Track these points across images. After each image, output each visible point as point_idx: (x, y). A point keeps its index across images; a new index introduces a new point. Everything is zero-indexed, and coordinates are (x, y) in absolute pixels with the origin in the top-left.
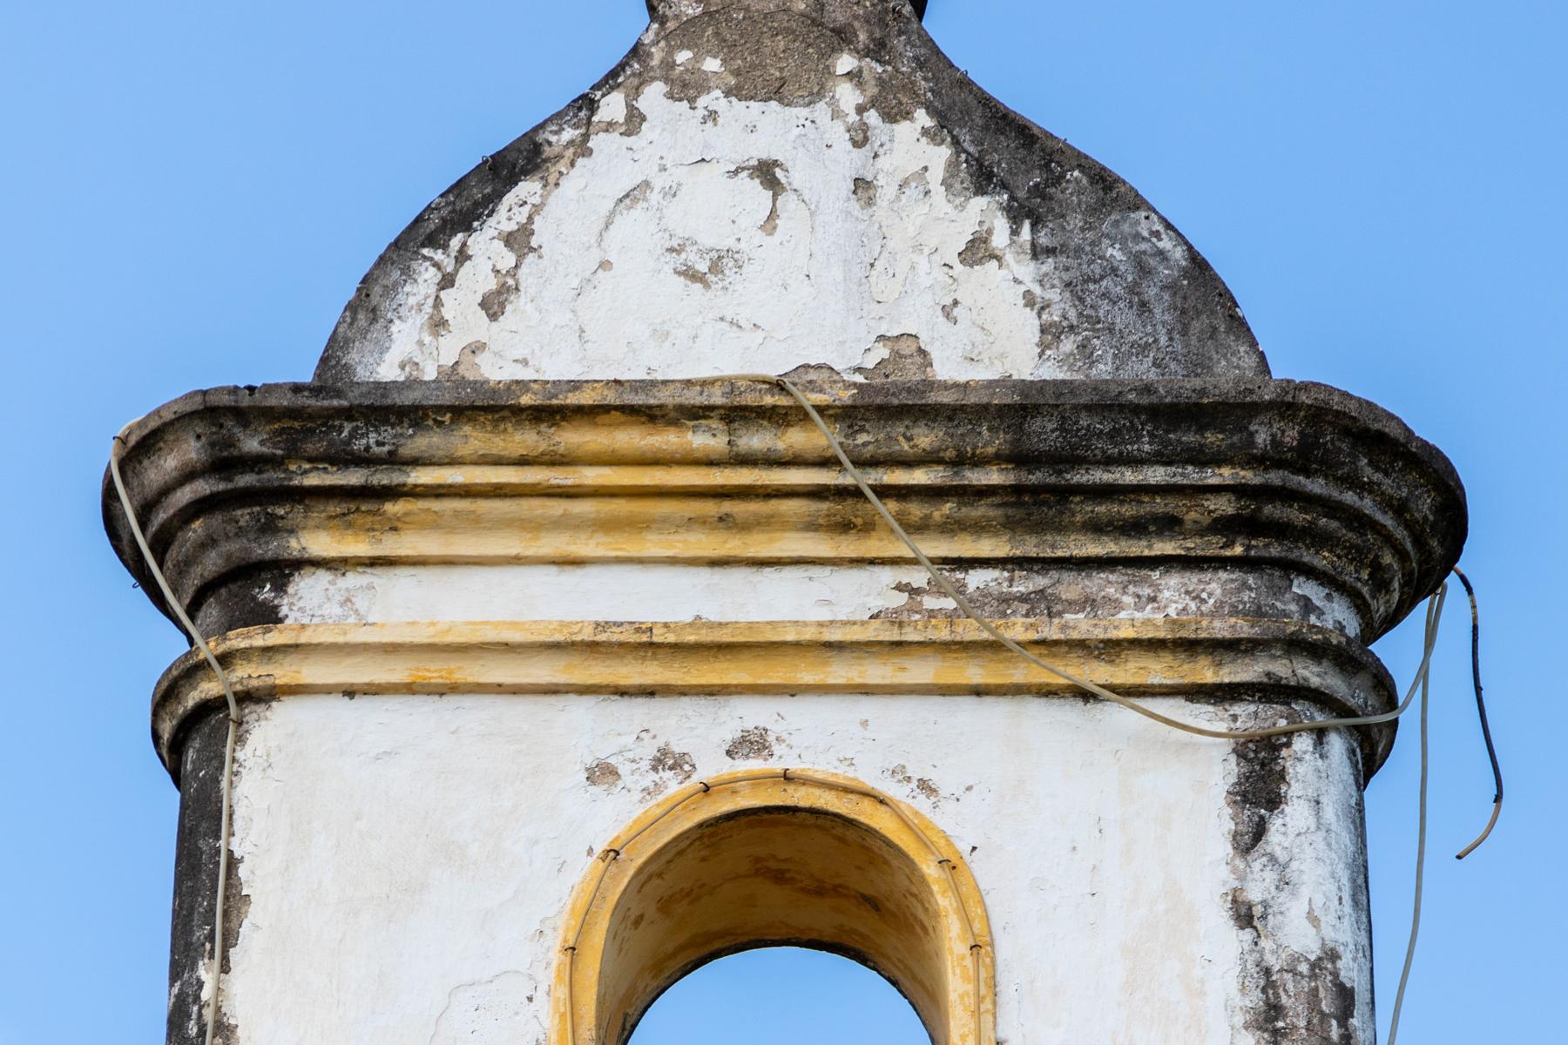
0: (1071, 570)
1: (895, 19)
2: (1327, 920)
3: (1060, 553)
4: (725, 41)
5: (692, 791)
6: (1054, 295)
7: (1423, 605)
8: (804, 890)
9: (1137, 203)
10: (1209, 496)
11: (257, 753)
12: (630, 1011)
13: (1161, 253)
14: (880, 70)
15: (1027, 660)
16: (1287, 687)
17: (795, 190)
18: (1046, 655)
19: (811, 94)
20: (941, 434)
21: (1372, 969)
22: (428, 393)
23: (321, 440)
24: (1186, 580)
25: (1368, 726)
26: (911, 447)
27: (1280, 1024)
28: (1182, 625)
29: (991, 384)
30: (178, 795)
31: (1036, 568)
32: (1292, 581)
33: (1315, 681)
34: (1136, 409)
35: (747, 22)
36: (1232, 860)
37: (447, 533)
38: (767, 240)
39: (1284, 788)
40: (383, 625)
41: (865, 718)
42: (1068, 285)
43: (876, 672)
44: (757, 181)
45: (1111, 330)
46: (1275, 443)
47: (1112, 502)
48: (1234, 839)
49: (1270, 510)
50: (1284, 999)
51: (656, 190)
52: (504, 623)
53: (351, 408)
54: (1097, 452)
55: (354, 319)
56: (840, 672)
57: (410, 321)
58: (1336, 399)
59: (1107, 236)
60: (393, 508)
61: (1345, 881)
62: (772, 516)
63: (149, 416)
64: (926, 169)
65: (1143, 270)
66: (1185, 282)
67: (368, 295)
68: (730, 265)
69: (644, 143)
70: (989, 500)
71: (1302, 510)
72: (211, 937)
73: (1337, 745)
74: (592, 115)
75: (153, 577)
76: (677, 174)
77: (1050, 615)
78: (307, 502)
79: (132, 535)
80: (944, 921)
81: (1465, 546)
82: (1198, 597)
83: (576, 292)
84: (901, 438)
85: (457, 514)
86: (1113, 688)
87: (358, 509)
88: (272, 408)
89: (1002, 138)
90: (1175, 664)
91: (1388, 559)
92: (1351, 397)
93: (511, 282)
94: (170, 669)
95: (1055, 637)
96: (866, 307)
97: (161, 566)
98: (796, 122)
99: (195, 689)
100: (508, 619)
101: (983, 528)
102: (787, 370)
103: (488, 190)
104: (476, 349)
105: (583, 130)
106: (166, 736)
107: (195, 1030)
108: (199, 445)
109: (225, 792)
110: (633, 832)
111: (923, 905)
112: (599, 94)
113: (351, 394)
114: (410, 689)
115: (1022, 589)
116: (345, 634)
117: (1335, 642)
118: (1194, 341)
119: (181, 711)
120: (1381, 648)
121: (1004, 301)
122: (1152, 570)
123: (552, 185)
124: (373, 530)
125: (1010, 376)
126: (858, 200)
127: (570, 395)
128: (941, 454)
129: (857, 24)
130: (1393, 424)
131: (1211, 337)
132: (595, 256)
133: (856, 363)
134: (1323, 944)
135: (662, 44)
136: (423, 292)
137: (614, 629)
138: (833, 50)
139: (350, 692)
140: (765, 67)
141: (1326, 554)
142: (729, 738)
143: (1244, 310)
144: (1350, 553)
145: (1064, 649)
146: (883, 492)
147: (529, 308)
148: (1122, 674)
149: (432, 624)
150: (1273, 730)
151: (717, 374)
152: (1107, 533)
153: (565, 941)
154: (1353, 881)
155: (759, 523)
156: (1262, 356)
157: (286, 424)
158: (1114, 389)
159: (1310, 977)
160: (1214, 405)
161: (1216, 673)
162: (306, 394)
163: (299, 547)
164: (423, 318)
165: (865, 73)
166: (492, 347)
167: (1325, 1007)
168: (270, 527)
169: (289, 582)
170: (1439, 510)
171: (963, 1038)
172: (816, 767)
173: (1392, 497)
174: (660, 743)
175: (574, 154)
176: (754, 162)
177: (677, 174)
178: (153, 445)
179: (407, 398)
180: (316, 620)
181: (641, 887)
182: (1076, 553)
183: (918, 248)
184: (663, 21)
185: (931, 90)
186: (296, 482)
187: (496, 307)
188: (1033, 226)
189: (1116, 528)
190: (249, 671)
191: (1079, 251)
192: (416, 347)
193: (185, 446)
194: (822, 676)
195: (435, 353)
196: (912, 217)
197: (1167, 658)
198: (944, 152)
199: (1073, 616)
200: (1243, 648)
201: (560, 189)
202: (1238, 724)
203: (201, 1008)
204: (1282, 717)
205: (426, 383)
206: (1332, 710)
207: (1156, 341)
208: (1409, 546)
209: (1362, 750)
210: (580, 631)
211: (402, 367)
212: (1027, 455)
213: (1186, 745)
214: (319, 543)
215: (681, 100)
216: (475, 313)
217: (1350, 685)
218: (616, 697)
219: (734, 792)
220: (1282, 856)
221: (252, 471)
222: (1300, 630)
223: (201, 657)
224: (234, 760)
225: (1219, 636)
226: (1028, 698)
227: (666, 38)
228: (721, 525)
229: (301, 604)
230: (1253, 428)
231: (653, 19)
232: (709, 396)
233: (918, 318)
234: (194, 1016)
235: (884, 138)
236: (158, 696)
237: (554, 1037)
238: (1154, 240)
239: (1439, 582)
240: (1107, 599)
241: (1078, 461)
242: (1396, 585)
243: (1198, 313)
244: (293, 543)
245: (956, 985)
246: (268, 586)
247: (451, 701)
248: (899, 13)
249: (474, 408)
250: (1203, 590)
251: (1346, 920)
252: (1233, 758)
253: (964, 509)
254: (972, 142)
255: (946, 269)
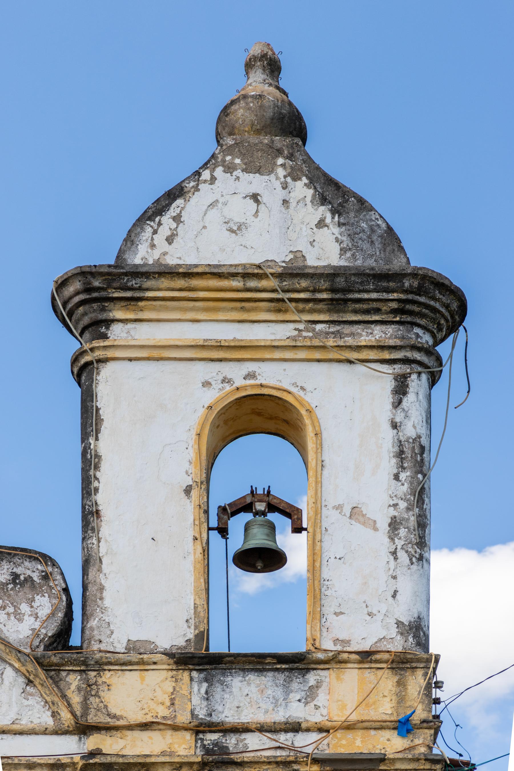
0: (347, 324)
1: (296, 146)
2: (418, 427)
3: (344, 319)
4: (242, 153)
5: (233, 389)
6: (344, 238)
7: (452, 336)
8: (267, 418)
9: (372, 209)
10: (390, 302)
11: (103, 377)
12: (216, 452)
13: (378, 225)
14: (291, 163)
15: (333, 351)
16: (410, 360)
17: (264, 203)
18: (339, 350)
19: (269, 171)
20: (309, 282)
21: (430, 441)
22: (150, 268)
23: (118, 282)
24: (382, 328)
25: (434, 371)
26: (300, 286)
27: (403, 456)
28: (380, 341)
29: (324, 267)
30: (80, 389)
31: (337, 324)
32: (413, 328)
33: (419, 358)
34: (369, 275)
35: (249, 147)
36: (392, 410)
37: (158, 311)
38: (255, 220)
39: (408, 389)
40: (139, 340)
41: (284, 368)
42: (349, 235)
43: (288, 355)
44: (252, 200)
45: (362, 250)
46: (411, 286)
47: (361, 304)
48: (393, 404)
49: (408, 307)
50: (405, 449)
51: (220, 203)
52: (176, 339)
53: (127, 272)
54: (356, 288)
55: (126, 244)
56: (278, 355)
57: (144, 245)
58: (430, 272)
59: (362, 220)
60: (141, 304)
61: (424, 416)
62: (257, 307)
63: (64, 274)
64: (305, 197)
65: (373, 231)
66: (385, 235)
67: (130, 236)
68: (244, 228)
69: (216, 187)
70: (323, 303)
71: (418, 307)
72: (92, 431)
73: (424, 377)
74: (199, 178)
75: (68, 324)
76: (227, 197)
77: (341, 338)
78: (114, 302)
79: (61, 311)
80: (307, 427)
81: (466, 318)
82: (385, 333)
83: (196, 236)
84: (296, 284)
85: (160, 306)
86: (359, 360)
87: (130, 304)
88: (102, 272)
89: (330, 187)
90: (377, 353)
91: (442, 322)
92: (435, 272)
93: (175, 232)
94: (75, 352)
95: (342, 345)
96: (286, 242)
97: (71, 321)
98: (264, 181)
99: (83, 358)
100: (177, 338)
101: (321, 311)
102: (261, 262)
103: (167, 202)
104: (165, 254)
105: (196, 183)
106: (75, 372)
107: (90, 457)
108: (80, 283)
109: (94, 389)
110: (216, 401)
111: (301, 422)
112: (201, 170)
113: (126, 268)
114: (148, 359)
115: (332, 330)
116: (128, 342)
117: (425, 347)
118: (387, 254)
119: (79, 365)
120: (439, 349)
121: (329, 240)
122: (372, 325)
123: (187, 201)
124: (135, 310)
125: (330, 264)
126: (284, 207)
127: (194, 269)
128: (309, 289)
129: (284, 148)
130: (447, 280)
131: (393, 253)
132: (201, 225)
133: (283, 259)
134: (417, 434)
135: (222, 154)
136: (148, 235)
137: (209, 341)
138: (276, 157)
139: (130, 360)
140: (254, 162)
141: (424, 320)
142: (244, 374)
143: (403, 244)
144: (431, 320)
145: (344, 348)
146: (291, 300)
147: (181, 241)
148: (362, 356)
149: (154, 339)
150: (405, 372)
151: (240, 263)
152: (359, 313)
153: (197, 432)
154: (427, 416)
155: (253, 310)
156: (408, 258)
157: (107, 277)
158: (362, 269)
159: (413, 443)
160: (393, 274)
161: (389, 356)
162: (112, 268)
163: (112, 315)
164: (148, 244)
165: (287, 164)
166: (170, 253)
167: (416, 451)
168: (103, 309)
169: (110, 326)
170: (459, 307)
171: (312, 460)
172: (270, 383)
173: (445, 303)
174: (224, 375)
175: (194, 190)
176: (251, 194)
177: (227, 197)
178: (66, 283)
179: (144, 270)
180: (119, 338)
181: (219, 417)
182: (349, 319)
183: (303, 223)
184: (222, 147)
185: (308, 171)
186: (111, 296)
187: (171, 240)
188: (339, 216)
189: (361, 312)
190: (100, 353)
191: (353, 224)
192: (146, 253)
193: (75, 284)
194: (272, 356)
195: (152, 255)
196: (301, 212)
197: (375, 351)
198: (311, 191)
199: (348, 338)
200: (398, 348)
201: (190, 202)
202: (395, 371)
203: (91, 450)
204: (408, 369)
205: (149, 265)
206: (423, 367)
207: (376, 253)
208: (449, 318)
209: (431, 378)
210: (199, 342)
211: (142, 259)
212: (335, 289)
213: (380, 377)
214: (118, 314)
215: (228, 173)
216: (164, 242)
217: (429, 359)
218: (211, 362)
219: (246, 390)
220: (406, 409)
221: (97, 292)
222: (415, 343)
223: (85, 349)
224: (96, 379)
225: (391, 345)
226: (333, 363)
227: (223, 152)
228: (241, 310)
229: (114, 333)
230: (404, 281)
231: (218, 145)
232: (237, 270)
233: (302, 246)
234: (89, 453)
235: (293, 186)
236: (72, 360)
237: (194, 459)
238: (376, 221)
239: (457, 329)
240: (358, 333)
241: (350, 291)
242: (444, 330)
243: (389, 245)
244: (111, 314)
245: (311, 445)
246: (104, 328)
247: (161, 362)
248: (298, 144)
249: (165, 273)
250: (387, 331)
251: (424, 427)
252: (393, 381)
253: (315, 306)
254: (320, 188)
255: (311, 230)
